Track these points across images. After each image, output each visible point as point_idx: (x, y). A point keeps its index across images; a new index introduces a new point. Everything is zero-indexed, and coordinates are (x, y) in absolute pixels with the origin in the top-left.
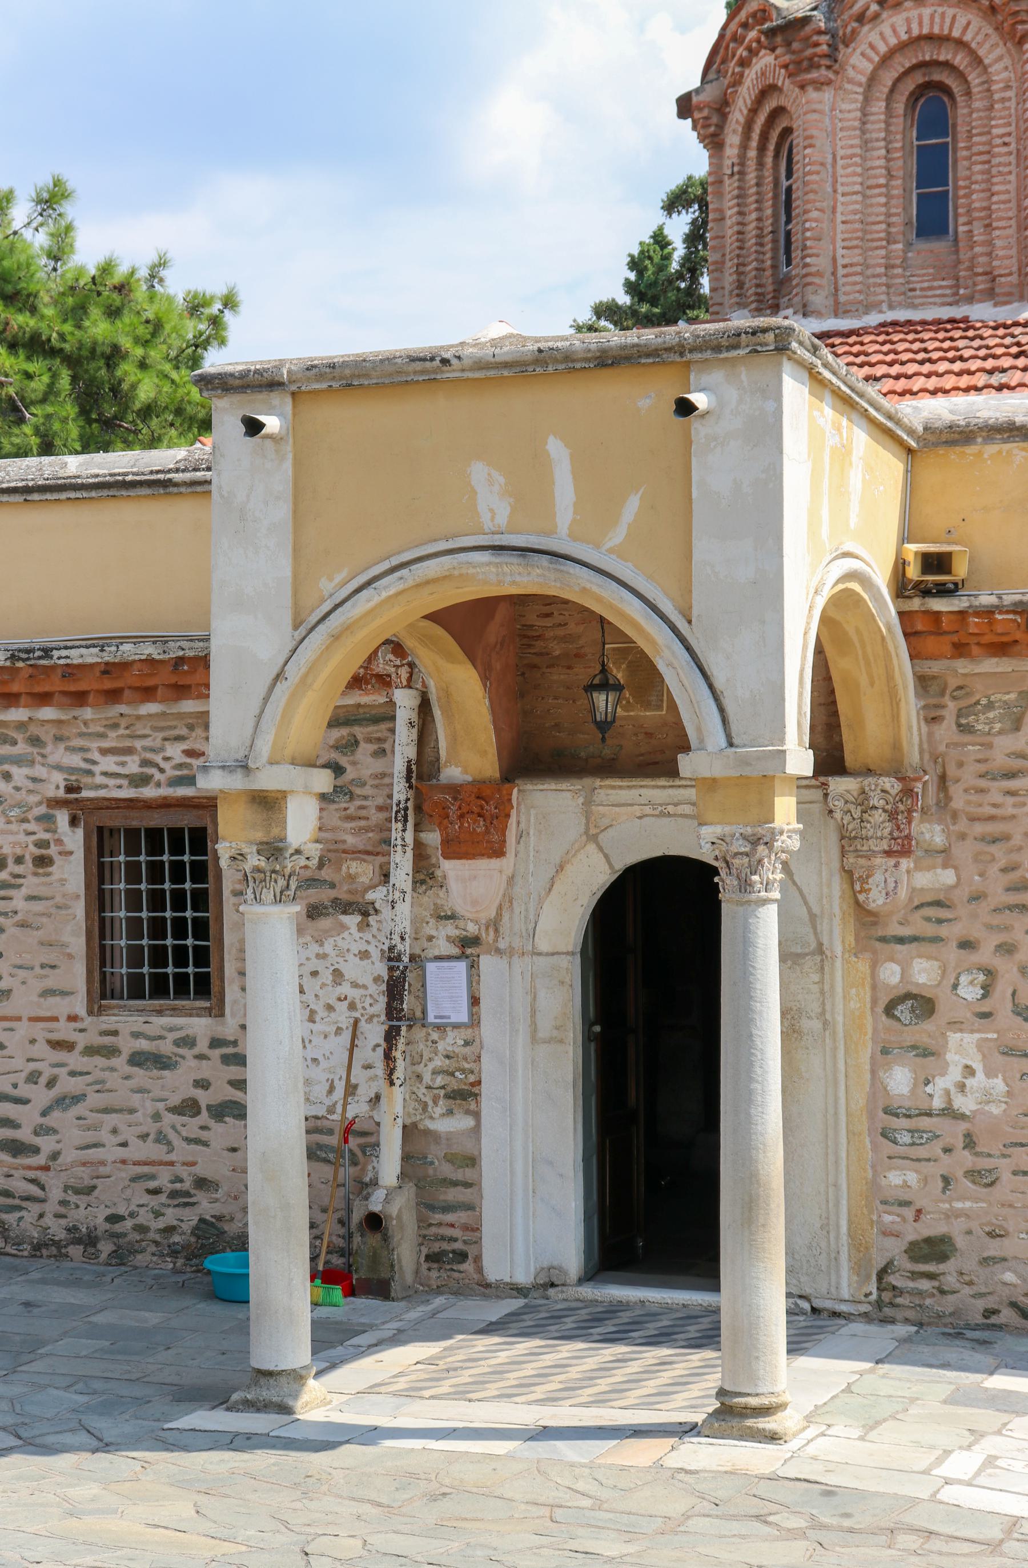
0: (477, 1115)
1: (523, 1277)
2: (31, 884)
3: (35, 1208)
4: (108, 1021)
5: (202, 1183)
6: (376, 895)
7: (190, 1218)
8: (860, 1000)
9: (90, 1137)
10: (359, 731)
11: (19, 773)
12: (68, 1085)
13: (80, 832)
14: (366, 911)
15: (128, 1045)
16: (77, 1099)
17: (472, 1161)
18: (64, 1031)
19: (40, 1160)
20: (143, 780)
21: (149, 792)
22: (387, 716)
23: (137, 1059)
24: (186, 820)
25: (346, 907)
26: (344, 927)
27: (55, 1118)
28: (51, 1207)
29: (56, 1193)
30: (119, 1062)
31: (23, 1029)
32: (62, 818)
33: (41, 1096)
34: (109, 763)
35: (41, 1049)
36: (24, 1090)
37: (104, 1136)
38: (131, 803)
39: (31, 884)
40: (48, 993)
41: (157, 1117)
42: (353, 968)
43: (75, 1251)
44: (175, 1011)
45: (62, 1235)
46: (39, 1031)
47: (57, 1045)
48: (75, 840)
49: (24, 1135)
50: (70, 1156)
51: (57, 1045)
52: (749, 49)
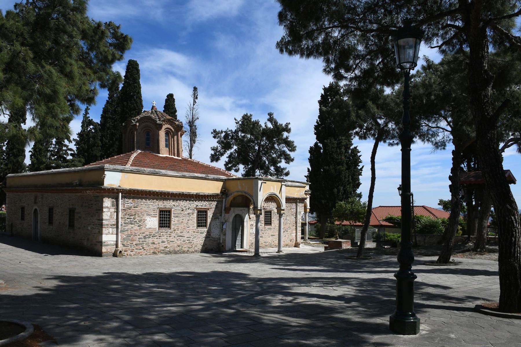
0: (226, 236)
1: (228, 250)
2: (192, 216)
3: (191, 248)
4: (198, 229)
5: (206, 244)
6: (219, 217)
7: (205, 247)
8: (249, 225)
9: (197, 241)
10: (219, 202)
11: (192, 205)
12: (195, 236)
13: (196, 211)
14: (219, 218)
15: (200, 232)
16: (195, 237)
17: (225, 240)
18: (195, 231)
19: (192, 243)
20: (202, 206)
21: (203, 207)
22: (222, 201)
23: (201, 233)
24: (205, 210)
25: (217, 218)
26: (217, 220)
27: (193, 239)
28: (193, 248)
29: (193, 247)
30: (199, 233)
31: (191, 231)
32: (195, 209)
33: (192, 237)
34: (200, 204)
35: (192, 232)
36: (191, 237)
37: (198, 240)
38: (201, 208)
39: (192, 216)
40: (193, 227)
41: (202, 238)
42: (218, 224)
43: (195, 252)
44: (204, 228)
45: (194, 251)
46: (192, 231)
47: (194, 232)
48: (196, 212)
49: (191, 241)
50: (195, 243)
51: (194, 232)
52: (145, 121)
